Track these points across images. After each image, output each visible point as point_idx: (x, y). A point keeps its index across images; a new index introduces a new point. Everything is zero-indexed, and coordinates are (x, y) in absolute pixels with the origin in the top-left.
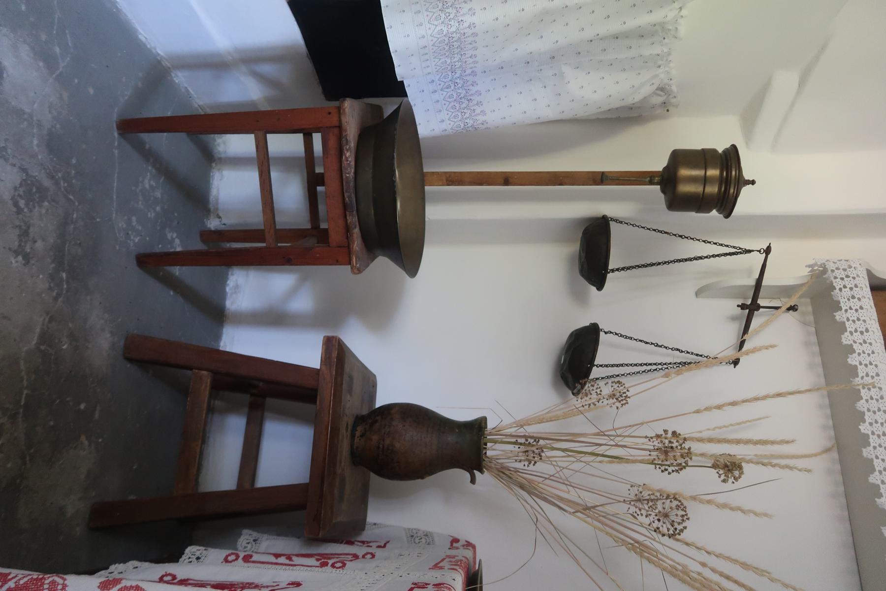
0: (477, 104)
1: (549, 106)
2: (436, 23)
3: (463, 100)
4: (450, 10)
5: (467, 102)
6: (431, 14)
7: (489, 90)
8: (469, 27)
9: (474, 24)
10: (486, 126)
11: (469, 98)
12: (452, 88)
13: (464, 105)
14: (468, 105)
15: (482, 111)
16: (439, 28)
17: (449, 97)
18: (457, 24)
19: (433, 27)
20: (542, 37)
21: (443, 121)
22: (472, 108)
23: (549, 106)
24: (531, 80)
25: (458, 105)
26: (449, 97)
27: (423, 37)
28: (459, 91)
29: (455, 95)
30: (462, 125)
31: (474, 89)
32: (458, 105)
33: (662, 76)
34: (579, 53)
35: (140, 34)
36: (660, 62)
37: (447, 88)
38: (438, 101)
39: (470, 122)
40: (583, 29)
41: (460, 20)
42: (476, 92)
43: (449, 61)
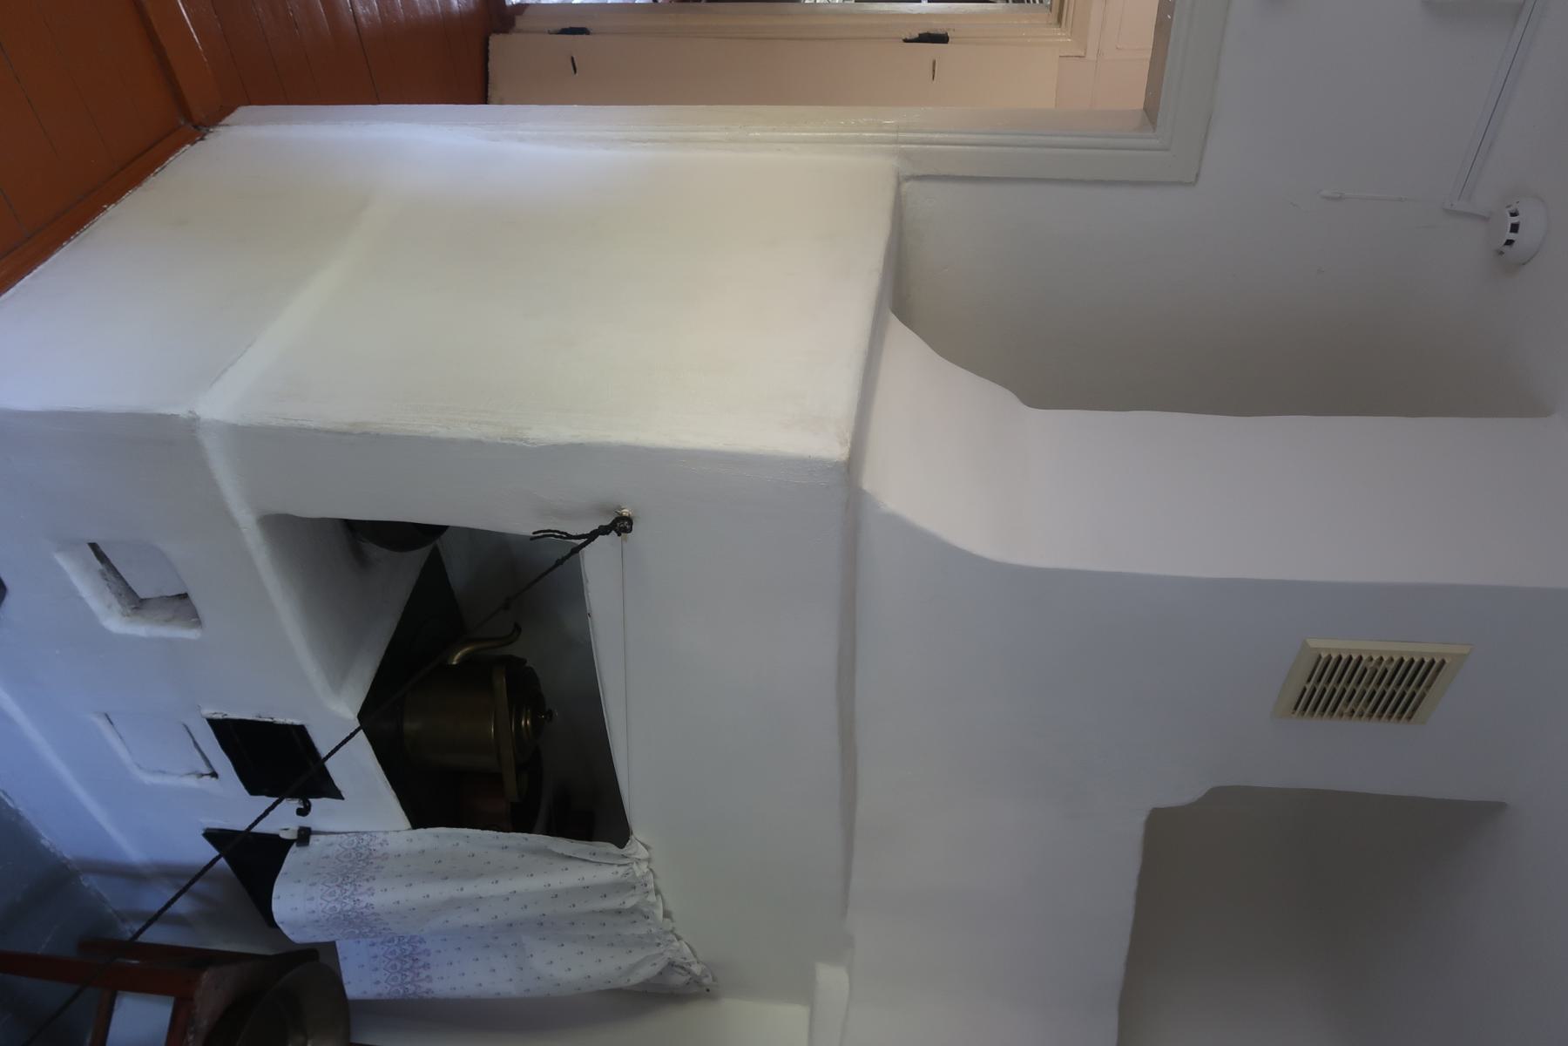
0: (424, 967)
1: (511, 980)
2: (329, 899)
3: (407, 959)
4: (347, 887)
5: (411, 962)
6: (325, 888)
7: (440, 952)
8: (366, 907)
9: (372, 905)
10: (430, 996)
11: (417, 957)
12: (396, 942)
13: (407, 966)
14: (411, 967)
15: (428, 977)
16: (331, 905)
17: (391, 953)
18: (352, 903)
19: (325, 903)
20: (478, 910)
21: (378, 982)
22: (416, 971)
23: (511, 980)
24: (488, 946)
25: (399, 965)
26: (391, 953)
27: (314, 912)
28: (404, 947)
29: (398, 951)
30: (401, 991)
31: (422, 947)
32: (399, 965)
33: (668, 955)
34: (542, 924)
35: (44, 838)
36: (658, 941)
37: (389, 942)
38: (376, 957)
39: (411, 988)
40: (526, 907)
41: (356, 899)
42: (425, 950)
43: (357, 932)
